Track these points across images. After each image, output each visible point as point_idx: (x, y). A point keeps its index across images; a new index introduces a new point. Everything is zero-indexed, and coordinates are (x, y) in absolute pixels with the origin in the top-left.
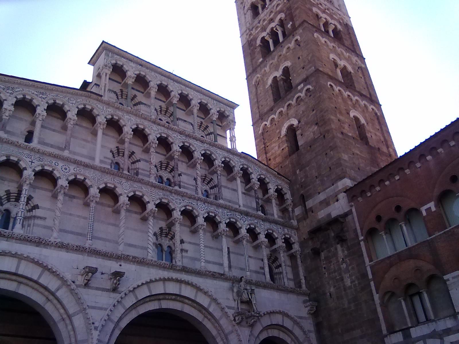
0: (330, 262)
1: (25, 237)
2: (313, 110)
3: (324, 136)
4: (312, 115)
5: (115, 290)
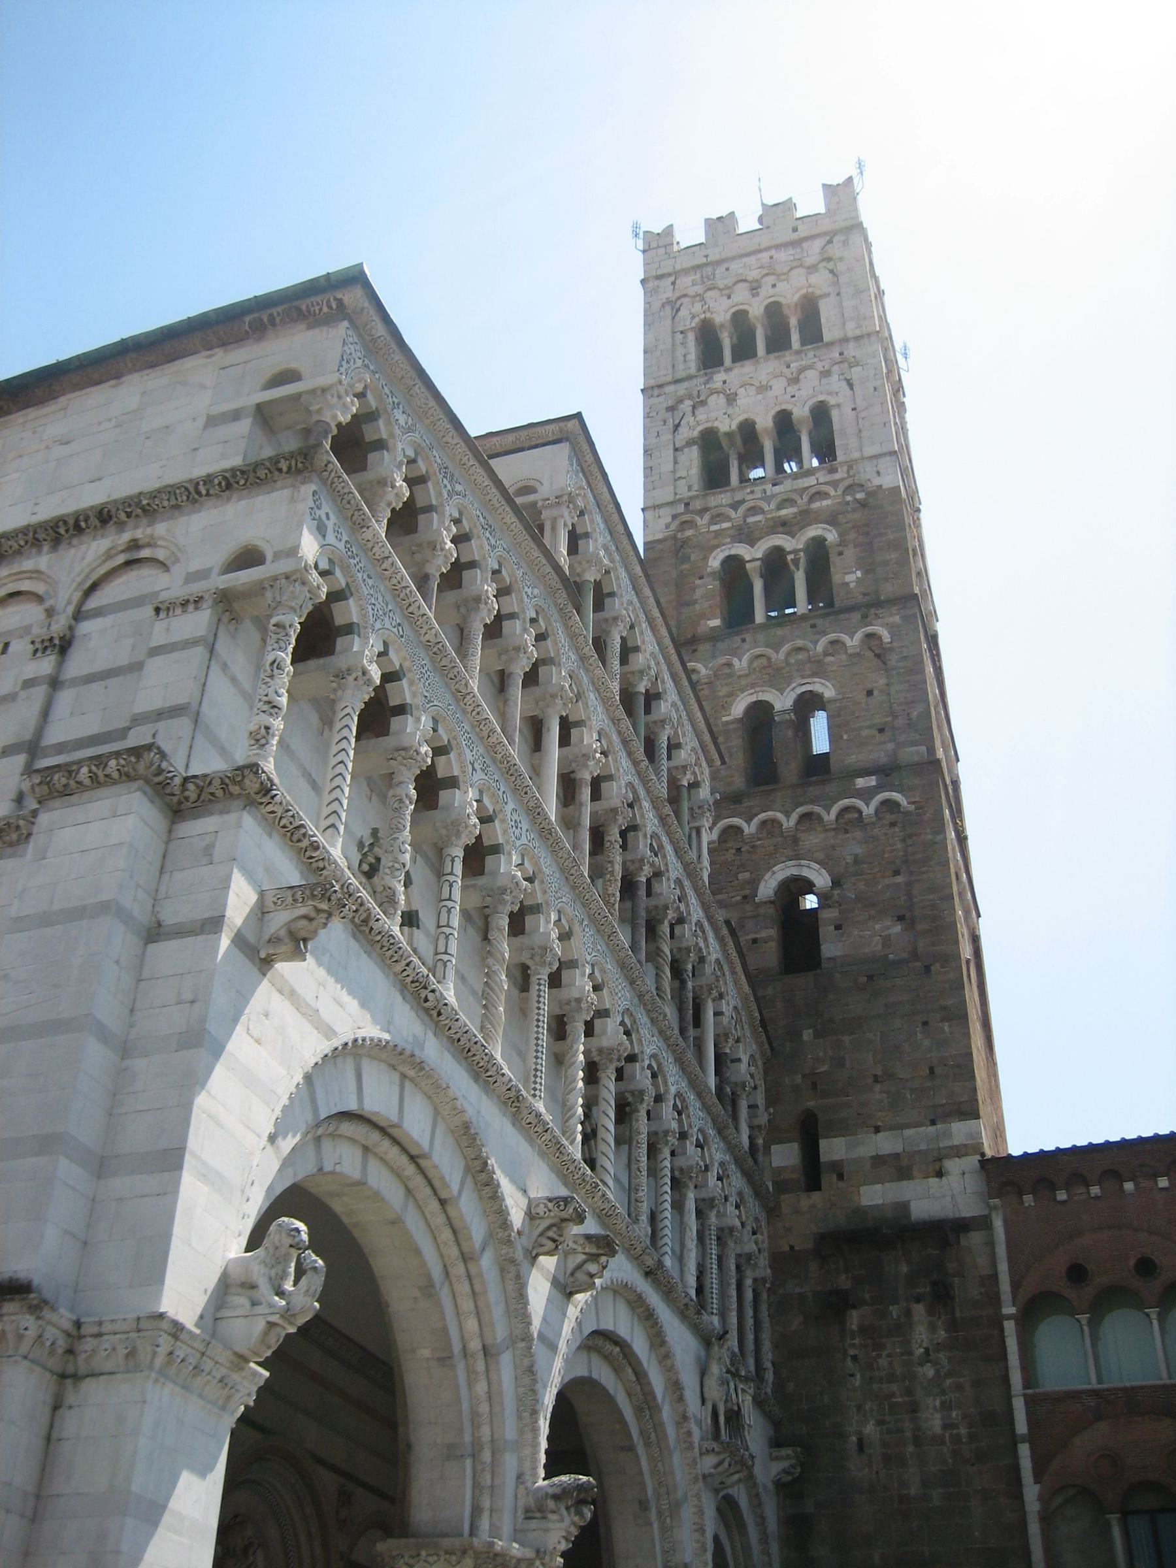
0: (879, 1347)
2: (897, 873)
3: (928, 969)
4: (888, 886)
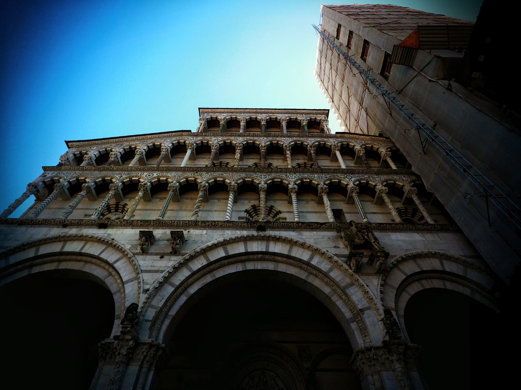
1: (92, 222)
5: (175, 252)
